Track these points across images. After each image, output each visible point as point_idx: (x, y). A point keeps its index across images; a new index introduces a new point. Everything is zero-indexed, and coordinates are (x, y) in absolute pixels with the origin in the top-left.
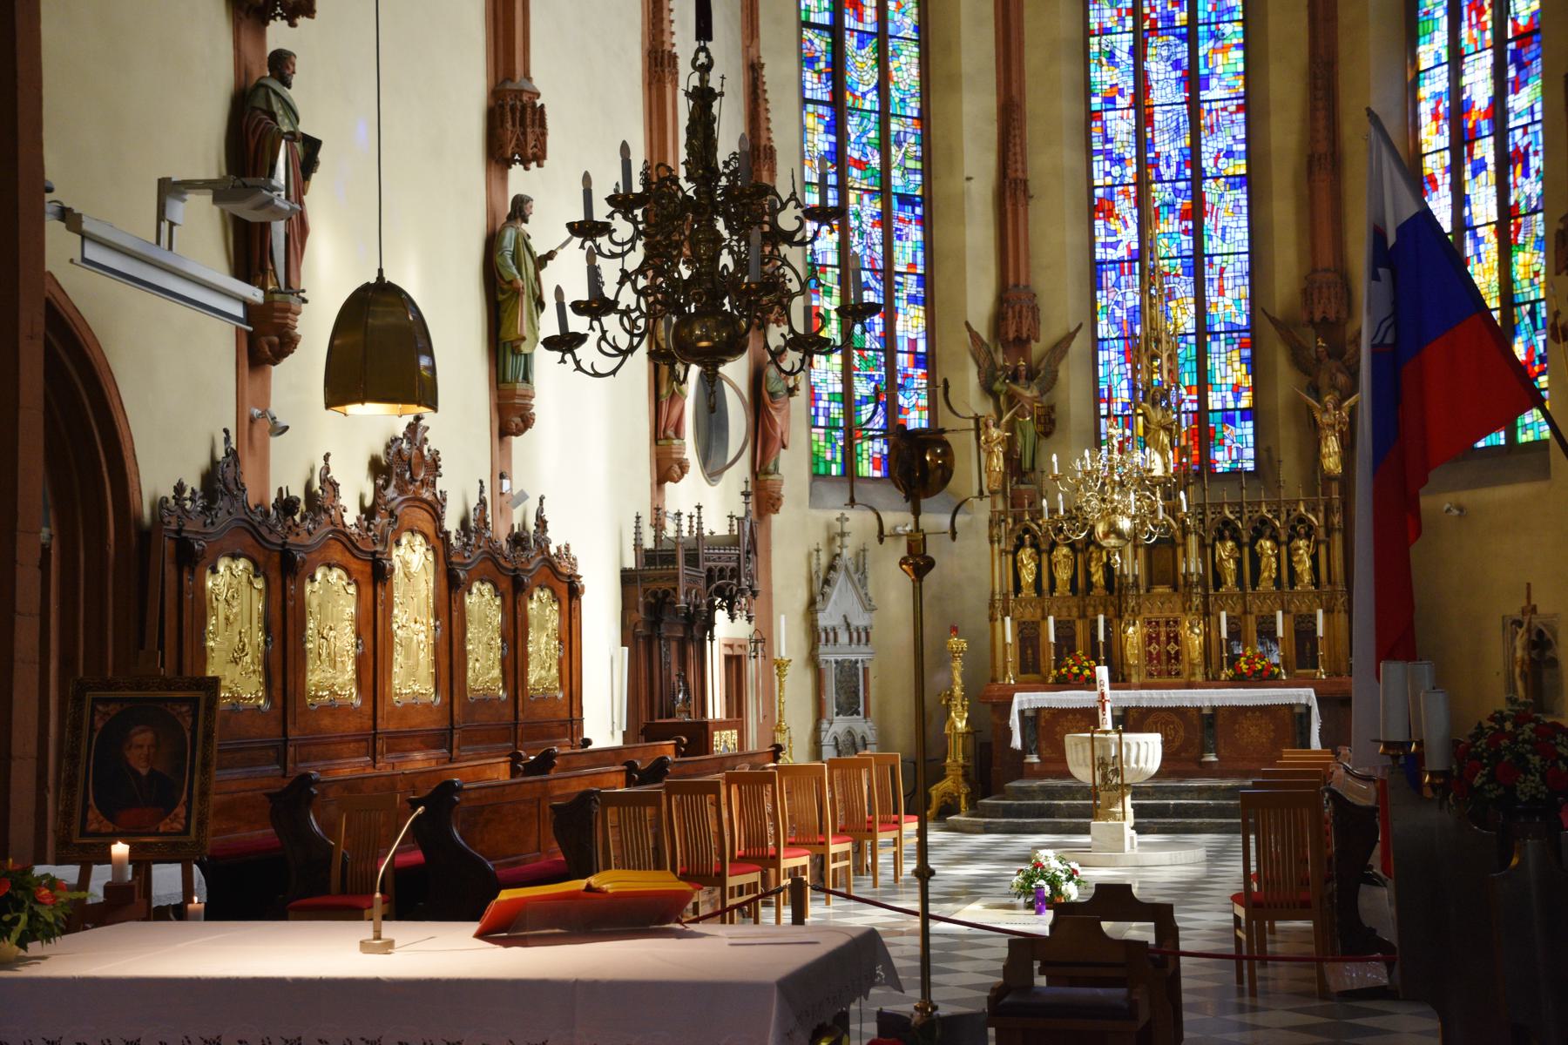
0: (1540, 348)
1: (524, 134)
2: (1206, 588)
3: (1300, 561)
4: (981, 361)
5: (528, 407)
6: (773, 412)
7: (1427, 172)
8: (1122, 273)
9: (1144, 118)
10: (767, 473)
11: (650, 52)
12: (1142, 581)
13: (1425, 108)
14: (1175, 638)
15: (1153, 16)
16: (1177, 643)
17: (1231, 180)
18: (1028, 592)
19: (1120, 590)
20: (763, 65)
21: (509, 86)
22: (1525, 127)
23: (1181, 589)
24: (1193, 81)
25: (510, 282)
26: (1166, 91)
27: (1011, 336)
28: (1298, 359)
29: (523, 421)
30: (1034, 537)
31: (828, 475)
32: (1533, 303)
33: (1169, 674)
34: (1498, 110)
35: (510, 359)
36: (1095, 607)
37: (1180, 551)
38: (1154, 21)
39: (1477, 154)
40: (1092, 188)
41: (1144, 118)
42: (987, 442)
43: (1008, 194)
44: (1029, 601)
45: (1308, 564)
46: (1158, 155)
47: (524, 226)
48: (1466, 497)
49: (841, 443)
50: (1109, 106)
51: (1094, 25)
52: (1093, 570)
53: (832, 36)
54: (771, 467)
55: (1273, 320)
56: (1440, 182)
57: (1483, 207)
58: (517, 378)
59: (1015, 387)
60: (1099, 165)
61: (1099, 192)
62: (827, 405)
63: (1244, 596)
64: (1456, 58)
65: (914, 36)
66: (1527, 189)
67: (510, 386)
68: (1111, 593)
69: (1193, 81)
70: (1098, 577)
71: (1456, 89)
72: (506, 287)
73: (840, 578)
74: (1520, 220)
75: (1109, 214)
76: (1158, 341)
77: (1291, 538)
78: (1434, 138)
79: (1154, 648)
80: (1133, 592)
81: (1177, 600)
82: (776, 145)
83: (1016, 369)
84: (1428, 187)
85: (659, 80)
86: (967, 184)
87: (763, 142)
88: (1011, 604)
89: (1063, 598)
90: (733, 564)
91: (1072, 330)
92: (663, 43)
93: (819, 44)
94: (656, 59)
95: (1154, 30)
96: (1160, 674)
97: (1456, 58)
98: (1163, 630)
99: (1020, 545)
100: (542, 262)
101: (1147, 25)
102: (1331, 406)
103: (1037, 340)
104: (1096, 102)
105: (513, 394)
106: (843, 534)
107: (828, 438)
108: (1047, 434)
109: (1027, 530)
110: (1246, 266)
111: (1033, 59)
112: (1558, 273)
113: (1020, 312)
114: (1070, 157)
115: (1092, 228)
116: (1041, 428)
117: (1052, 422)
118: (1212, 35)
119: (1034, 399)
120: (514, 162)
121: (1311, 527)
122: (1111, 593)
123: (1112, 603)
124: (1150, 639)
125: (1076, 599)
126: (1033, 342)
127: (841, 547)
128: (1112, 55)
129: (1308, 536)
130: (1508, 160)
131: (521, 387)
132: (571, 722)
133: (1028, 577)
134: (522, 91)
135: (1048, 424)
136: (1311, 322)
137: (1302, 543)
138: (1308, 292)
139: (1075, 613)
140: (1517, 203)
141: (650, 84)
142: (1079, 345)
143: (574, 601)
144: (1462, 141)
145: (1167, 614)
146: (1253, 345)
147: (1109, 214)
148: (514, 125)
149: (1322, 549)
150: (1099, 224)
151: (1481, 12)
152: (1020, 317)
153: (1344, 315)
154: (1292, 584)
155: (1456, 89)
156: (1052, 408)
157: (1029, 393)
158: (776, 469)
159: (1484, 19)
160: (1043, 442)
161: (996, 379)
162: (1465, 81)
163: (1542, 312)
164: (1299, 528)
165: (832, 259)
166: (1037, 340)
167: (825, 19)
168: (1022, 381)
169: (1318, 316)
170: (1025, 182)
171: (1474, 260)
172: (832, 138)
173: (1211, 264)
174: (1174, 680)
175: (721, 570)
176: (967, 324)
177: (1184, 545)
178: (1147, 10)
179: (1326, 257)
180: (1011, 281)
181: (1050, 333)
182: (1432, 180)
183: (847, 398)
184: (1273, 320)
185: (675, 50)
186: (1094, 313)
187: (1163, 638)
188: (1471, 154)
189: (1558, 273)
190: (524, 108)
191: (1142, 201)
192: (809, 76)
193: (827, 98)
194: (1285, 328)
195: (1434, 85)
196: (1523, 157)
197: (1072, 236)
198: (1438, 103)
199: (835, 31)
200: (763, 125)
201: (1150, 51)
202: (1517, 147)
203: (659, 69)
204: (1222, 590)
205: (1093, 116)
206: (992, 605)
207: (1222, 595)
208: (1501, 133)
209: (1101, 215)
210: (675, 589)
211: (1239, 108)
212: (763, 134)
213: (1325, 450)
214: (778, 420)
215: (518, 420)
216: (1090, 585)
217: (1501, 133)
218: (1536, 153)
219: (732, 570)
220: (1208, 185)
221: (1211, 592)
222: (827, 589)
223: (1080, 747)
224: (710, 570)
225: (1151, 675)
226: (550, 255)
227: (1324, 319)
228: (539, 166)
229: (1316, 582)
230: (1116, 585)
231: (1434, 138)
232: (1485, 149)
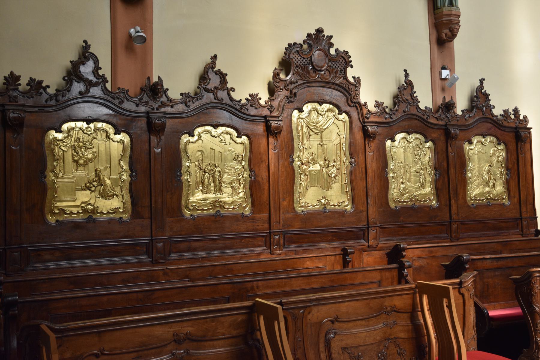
29: (450, 31)
58: (444, 6)
67: (440, 11)
131: (453, 10)
132: (521, 219)
143: (519, 144)
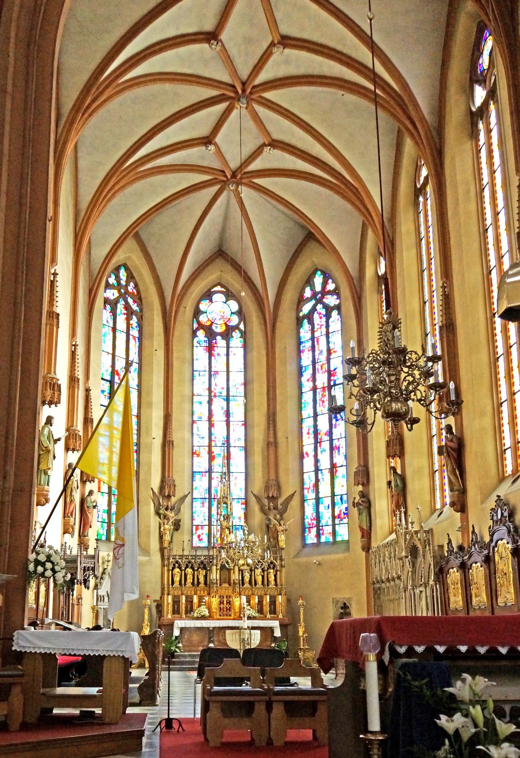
0: (344, 510)
1: (54, 393)
2: (240, 585)
3: (270, 577)
4: (155, 502)
5: (47, 495)
6: (88, 514)
7: (305, 451)
8: (202, 476)
9: (211, 425)
10: (85, 536)
11: (70, 376)
12: (218, 581)
13: (305, 431)
14: (229, 603)
15: (215, 391)
16: (230, 604)
17: (240, 448)
18: (177, 584)
19: (210, 585)
20: (91, 390)
21: (49, 375)
22: (338, 439)
23: (232, 585)
24: (228, 414)
25: (46, 447)
26: (219, 416)
27: (166, 494)
28: (262, 510)
30: (179, 565)
31: (101, 540)
32: (341, 495)
33: (227, 615)
34: (330, 433)
35: (43, 476)
36: (200, 591)
37: (232, 571)
38: (215, 394)
39: (322, 447)
40: (193, 446)
41: (211, 425)
42: (164, 530)
43: (167, 445)
44: (177, 588)
45: (273, 578)
46: (215, 438)
47: (50, 427)
48: (320, 558)
49: (106, 528)
50: (200, 419)
51: (195, 393)
52: (200, 577)
53: (110, 384)
54: (86, 534)
55: (254, 495)
56: (309, 455)
57: (325, 463)
59: (166, 512)
60: (195, 438)
61: (195, 448)
62: (102, 514)
63: (252, 588)
64: (316, 416)
65: (137, 388)
66: (339, 459)
67: (41, 487)
68: (206, 586)
69: (228, 414)
70: (202, 580)
71: (315, 426)
72: (44, 449)
73: (106, 577)
74: (337, 468)
75: (198, 455)
76: (227, 498)
77: (268, 569)
78: (308, 441)
79: (222, 606)
80: (215, 585)
81: (231, 589)
82: (93, 417)
83: (167, 506)
84: (305, 456)
85: (73, 387)
86: (153, 440)
87: (90, 417)
88: (171, 589)
89: (189, 587)
90: (93, 566)
91: (186, 494)
92: (75, 374)
93: (106, 386)
94: (72, 379)
95: (215, 396)
96: (223, 616)
97: (316, 416)
98: (225, 600)
99: (173, 569)
100: (56, 441)
101: (213, 394)
102: (282, 524)
103: (174, 496)
104: (195, 418)
105: (43, 490)
106: (109, 561)
107: (102, 527)
108: (177, 530)
109: (177, 562)
110: (244, 478)
111: (176, 400)
112: (355, 485)
113: (170, 486)
114: (187, 435)
115: (193, 459)
116: (175, 528)
117: (180, 525)
118: (235, 400)
119: (173, 517)
120: (46, 404)
121: (274, 565)
123: (206, 590)
124: (221, 603)
125: (194, 588)
126: (172, 497)
127: (107, 566)
128: (201, 403)
129: (273, 568)
130: (332, 449)
133: (177, 579)
134: (53, 378)
135: (177, 526)
136: (268, 497)
137: (272, 571)
138: (267, 488)
139: (193, 593)
140: (336, 464)
141: (69, 388)
142: (188, 500)
144: (317, 442)
145: (227, 594)
146: (246, 503)
147: (198, 455)
148: (50, 390)
149: (278, 573)
150: (194, 458)
151: (323, 402)
152: (170, 488)
153: (278, 495)
154: (268, 585)
155: (315, 426)
156: (180, 520)
157: (171, 514)
158: (88, 535)
159: (324, 404)
160: (175, 532)
161: (160, 509)
162: (318, 423)
163: (345, 498)
164: (272, 566)
165: (106, 462)
166: (174, 496)
168: (169, 510)
169: (270, 495)
170: (173, 442)
171: (321, 480)
173: (232, 476)
174: (228, 617)
175: (88, 567)
176: (152, 489)
177: (234, 569)
178: (213, 389)
179: (273, 476)
180: (167, 476)
181: (179, 494)
182: (307, 454)
183: (109, 512)
184: (254, 495)
185: (79, 377)
186: (192, 489)
187: (225, 602)
188: (320, 446)
189: (355, 485)
190: (54, 384)
191: (210, 452)
192: (102, 396)
194: (258, 499)
195: (308, 424)
196: (338, 448)
197: (187, 462)
198: (309, 429)
199: (111, 382)
200: (90, 410)
201: (213, 403)
202: (336, 446)
203: (73, 382)
205: (193, 422)
206: (163, 589)
208: (331, 440)
209: (196, 455)
210: (76, 573)
211: (243, 425)
212: (90, 413)
213: (280, 539)
214: (89, 516)
215: (44, 500)
216: (199, 583)
217: (331, 440)
218: (342, 448)
219: (92, 568)
220: (231, 449)
221: (241, 586)
222: (102, 581)
223: (234, 635)
224: (85, 567)
225: (220, 615)
226: (59, 439)
227: (273, 496)
228: (56, 406)
229: (276, 585)
230: (208, 583)
231: (308, 441)
232: (326, 445)
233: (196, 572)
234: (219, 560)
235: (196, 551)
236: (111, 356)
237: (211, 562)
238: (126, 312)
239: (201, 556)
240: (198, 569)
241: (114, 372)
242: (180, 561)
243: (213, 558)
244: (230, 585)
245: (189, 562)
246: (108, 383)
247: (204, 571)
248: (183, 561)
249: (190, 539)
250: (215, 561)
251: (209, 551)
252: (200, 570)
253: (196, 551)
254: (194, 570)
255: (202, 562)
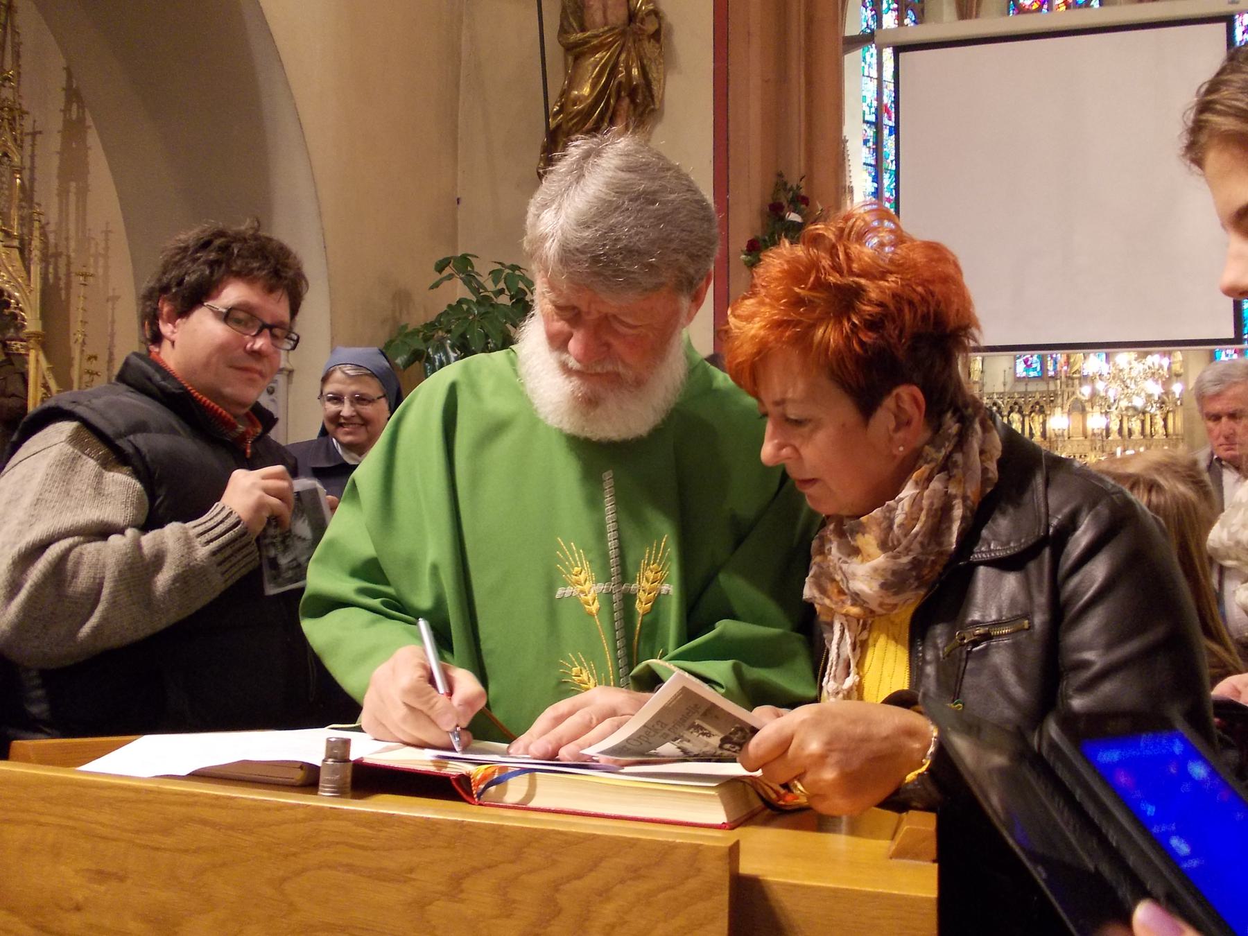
23: (1089, 438)
53: (876, 128)
68: (1045, 439)
82: (853, 184)
87: (848, 184)
93: (871, 132)
122: (1045, 439)
167: (872, 118)
172: (876, 185)
193: (873, 162)
199: (878, 125)
204: (1110, 438)
207: (1111, 441)
212: (847, 178)
221: (1105, 439)
233: (1027, 419)
234: (1066, 397)
235: (1026, 384)
236: (875, 81)
237: (1052, 401)
238: (895, 6)
239: (1035, 392)
240: (1031, 412)
241: (880, 110)
242: (1000, 402)
243: (1056, 395)
244: (1086, 438)
245: (1016, 403)
246: (873, 127)
247: (1041, 416)
248: (1005, 402)
249: (1013, 366)
250: (1059, 400)
251: (1048, 384)
252: (1033, 414)
253: (1026, 384)
254: (1023, 416)
255: (1037, 403)
